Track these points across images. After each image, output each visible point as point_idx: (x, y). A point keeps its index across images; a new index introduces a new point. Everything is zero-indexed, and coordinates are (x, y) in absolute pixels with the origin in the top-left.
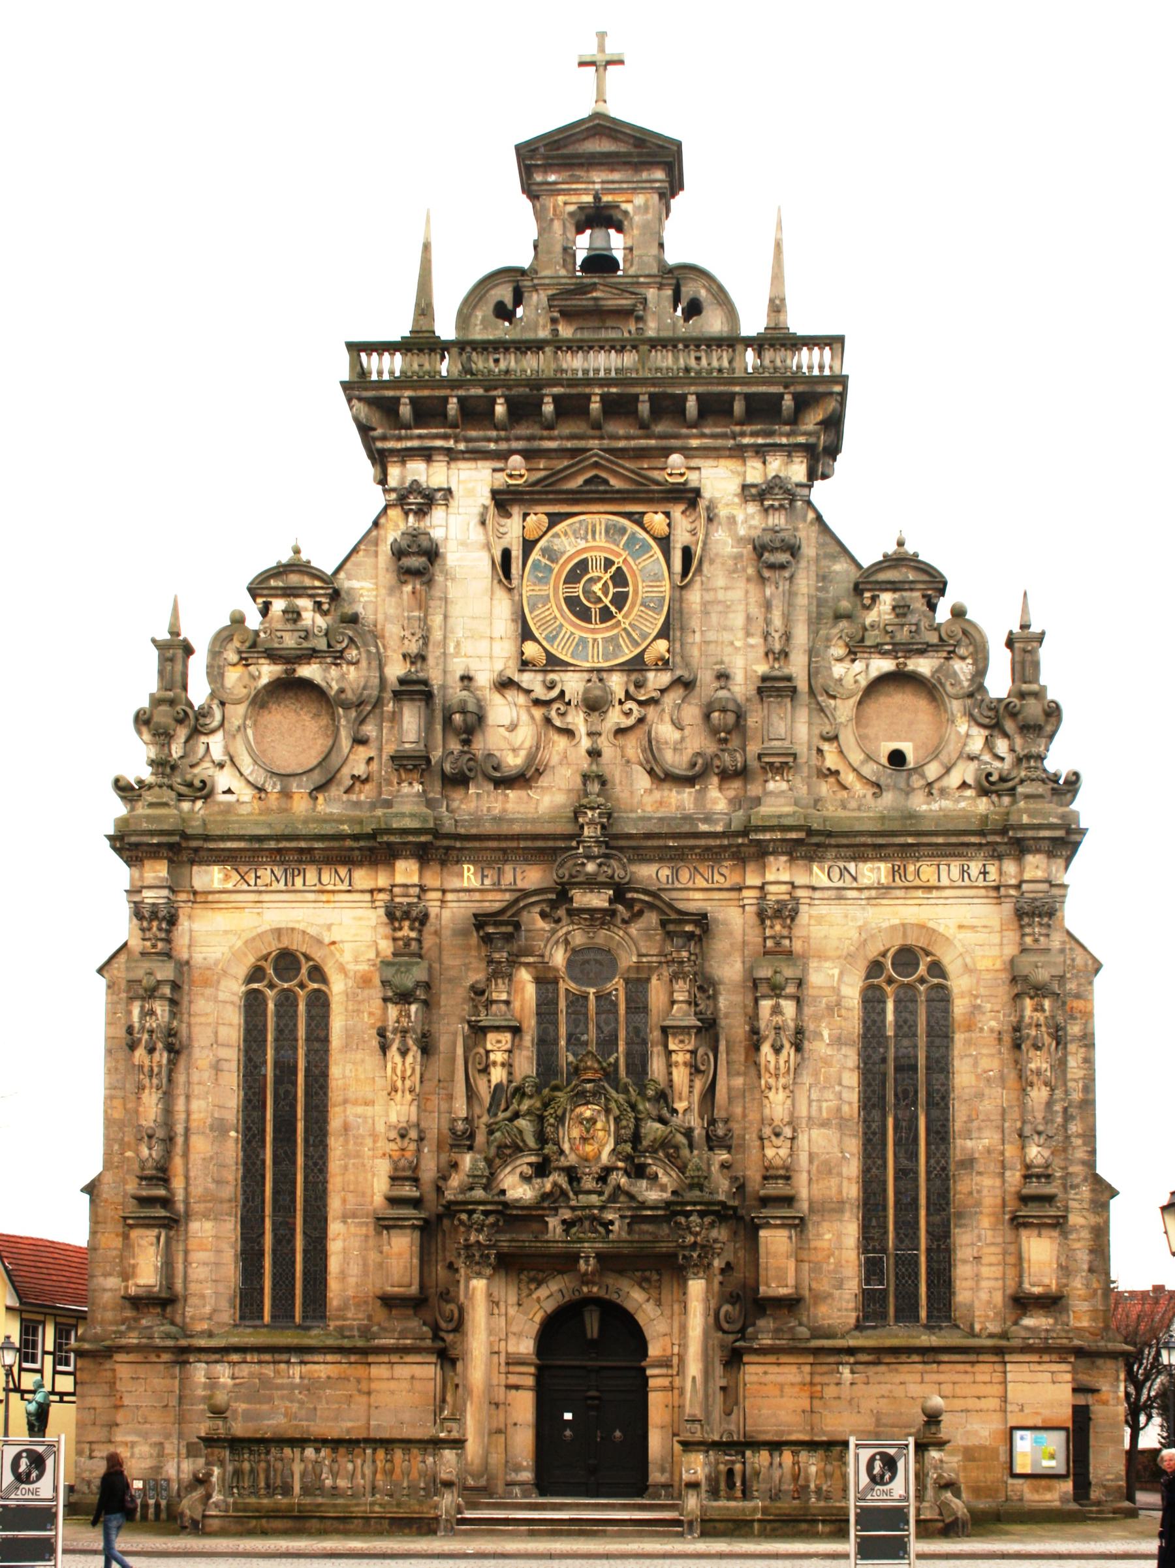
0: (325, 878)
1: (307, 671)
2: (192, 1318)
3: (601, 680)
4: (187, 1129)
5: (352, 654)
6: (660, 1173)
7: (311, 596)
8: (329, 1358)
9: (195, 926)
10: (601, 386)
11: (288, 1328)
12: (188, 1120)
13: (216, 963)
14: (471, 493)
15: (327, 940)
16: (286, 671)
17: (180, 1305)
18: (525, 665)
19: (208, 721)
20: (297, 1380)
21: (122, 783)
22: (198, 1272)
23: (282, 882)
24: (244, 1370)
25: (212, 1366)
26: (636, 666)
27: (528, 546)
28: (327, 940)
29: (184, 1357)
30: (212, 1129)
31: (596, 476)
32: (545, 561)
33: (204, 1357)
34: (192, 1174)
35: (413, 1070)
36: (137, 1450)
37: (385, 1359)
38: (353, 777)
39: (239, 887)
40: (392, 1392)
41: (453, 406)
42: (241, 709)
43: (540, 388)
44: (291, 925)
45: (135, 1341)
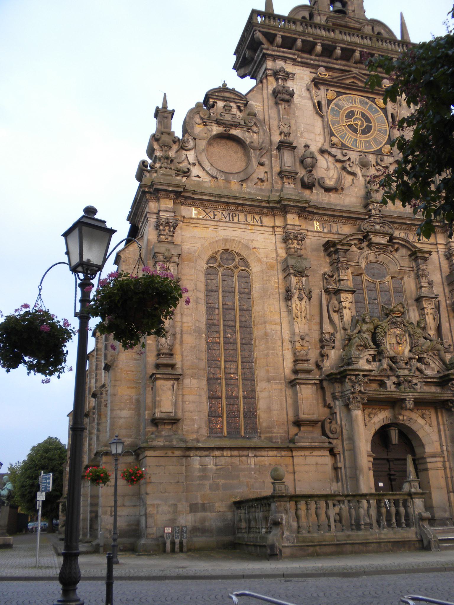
0: (249, 219)
1: (235, 132)
2: (187, 432)
3: (365, 156)
4: (182, 331)
5: (255, 129)
6: (431, 362)
7: (235, 103)
8: (271, 453)
9: (183, 233)
10: (360, 48)
11: (238, 438)
12: (182, 326)
13: (195, 251)
14: (302, 78)
15: (251, 247)
16: (225, 131)
17: (180, 424)
18: (333, 145)
19: (187, 145)
20: (253, 466)
21: (145, 164)
22: (190, 407)
23: (228, 218)
24: (222, 461)
25: (203, 458)
26: (378, 153)
27: (329, 102)
28: (251, 247)
29: (188, 453)
30: (195, 332)
31: (353, 82)
32: (336, 108)
33: (198, 453)
34: (184, 354)
35: (306, 307)
36: (160, 509)
37: (302, 453)
38: (258, 178)
39: (205, 218)
40: (307, 472)
41: (299, 43)
42: (204, 143)
43: (336, 43)
44: (233, 238)
45: (161, 444)
